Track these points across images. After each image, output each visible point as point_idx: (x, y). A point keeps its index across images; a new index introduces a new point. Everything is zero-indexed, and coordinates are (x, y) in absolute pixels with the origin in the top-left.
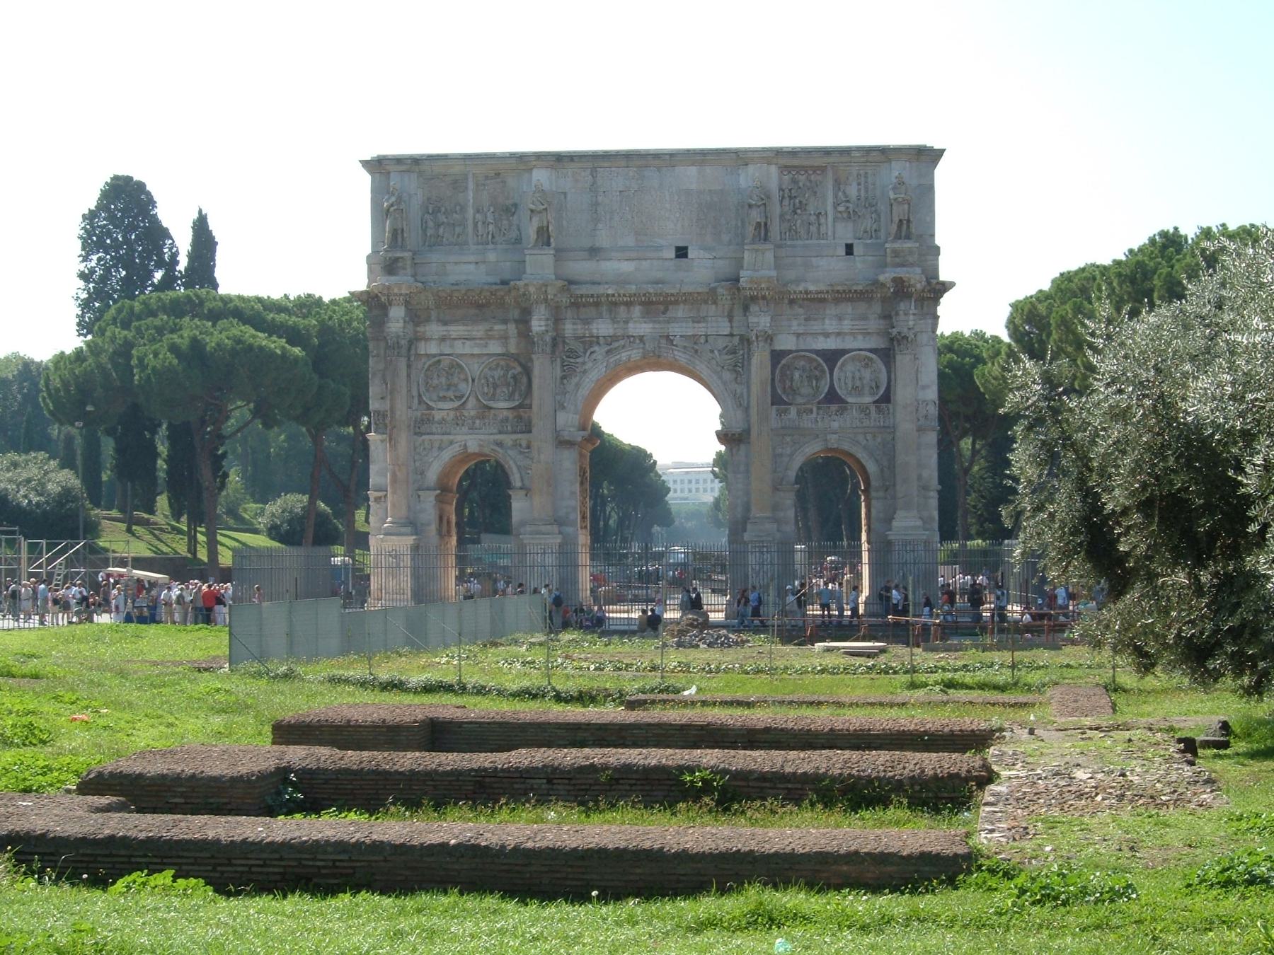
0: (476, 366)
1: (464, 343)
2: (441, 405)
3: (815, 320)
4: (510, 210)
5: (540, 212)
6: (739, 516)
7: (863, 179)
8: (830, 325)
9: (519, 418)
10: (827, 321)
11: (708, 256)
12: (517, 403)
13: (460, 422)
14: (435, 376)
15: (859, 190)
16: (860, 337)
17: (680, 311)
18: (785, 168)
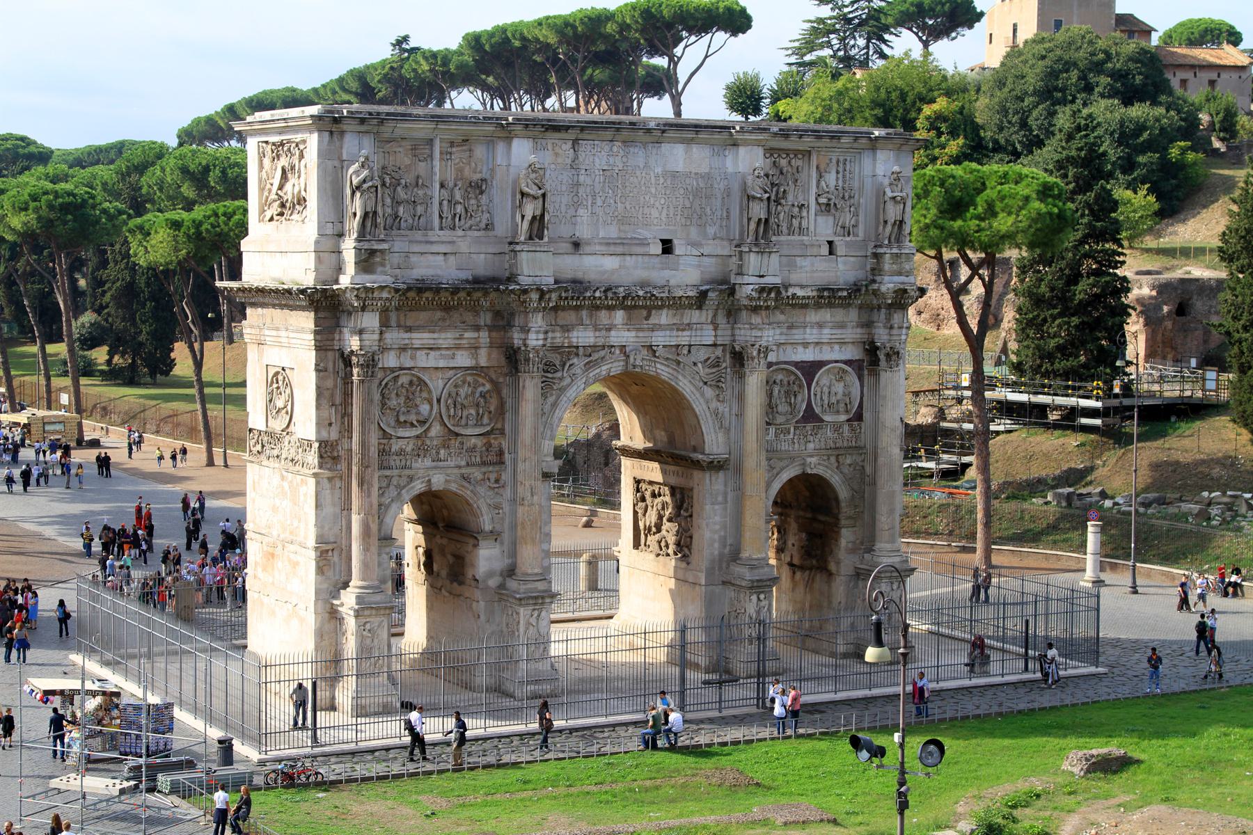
0: (441, 383)
1: (428, 354)
3: (797, 327)
4: (479, 187)
5: (535, 198)
6: (716, 552)
7: (841, 165)
8: (811, 335)
9: (488, 446)
10: (808, 330)
11: (695, 252)
12: (489, 428)
13: (422, 453)
14: (393, 396)
15: (837, 179)
16: (837, 347)
17: (664, 317)
18: (770, 152)
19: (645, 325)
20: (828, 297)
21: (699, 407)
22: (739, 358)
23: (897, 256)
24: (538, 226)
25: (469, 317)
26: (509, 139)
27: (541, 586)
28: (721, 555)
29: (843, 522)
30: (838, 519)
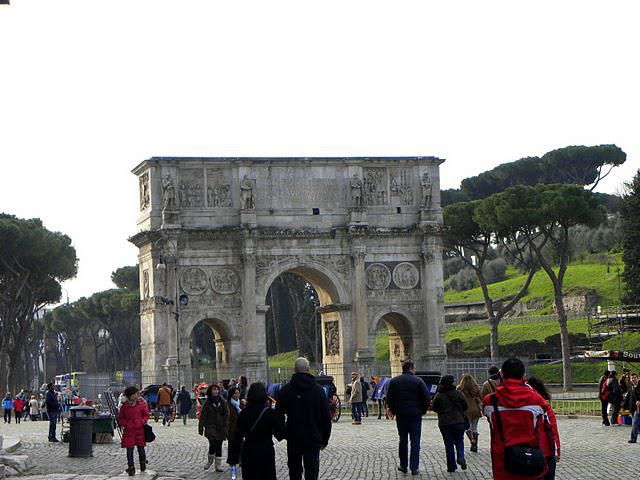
0: (211, 272)
2: (193, 293)
4: (226, 189)
8: (391, 249)
9: (234, 299)
17: (316, 242)
18: (366, 168)
19: (307, 245)
20: (397, 232)
21: (335, 282)
22: (352, 259)
23: (428, 212)
24: (250, 202)
25: (222, 243)
26: (238, 167)
27: (256, 358)
28: (351, 349)
29: (414, 336)
30: (411, 334)
